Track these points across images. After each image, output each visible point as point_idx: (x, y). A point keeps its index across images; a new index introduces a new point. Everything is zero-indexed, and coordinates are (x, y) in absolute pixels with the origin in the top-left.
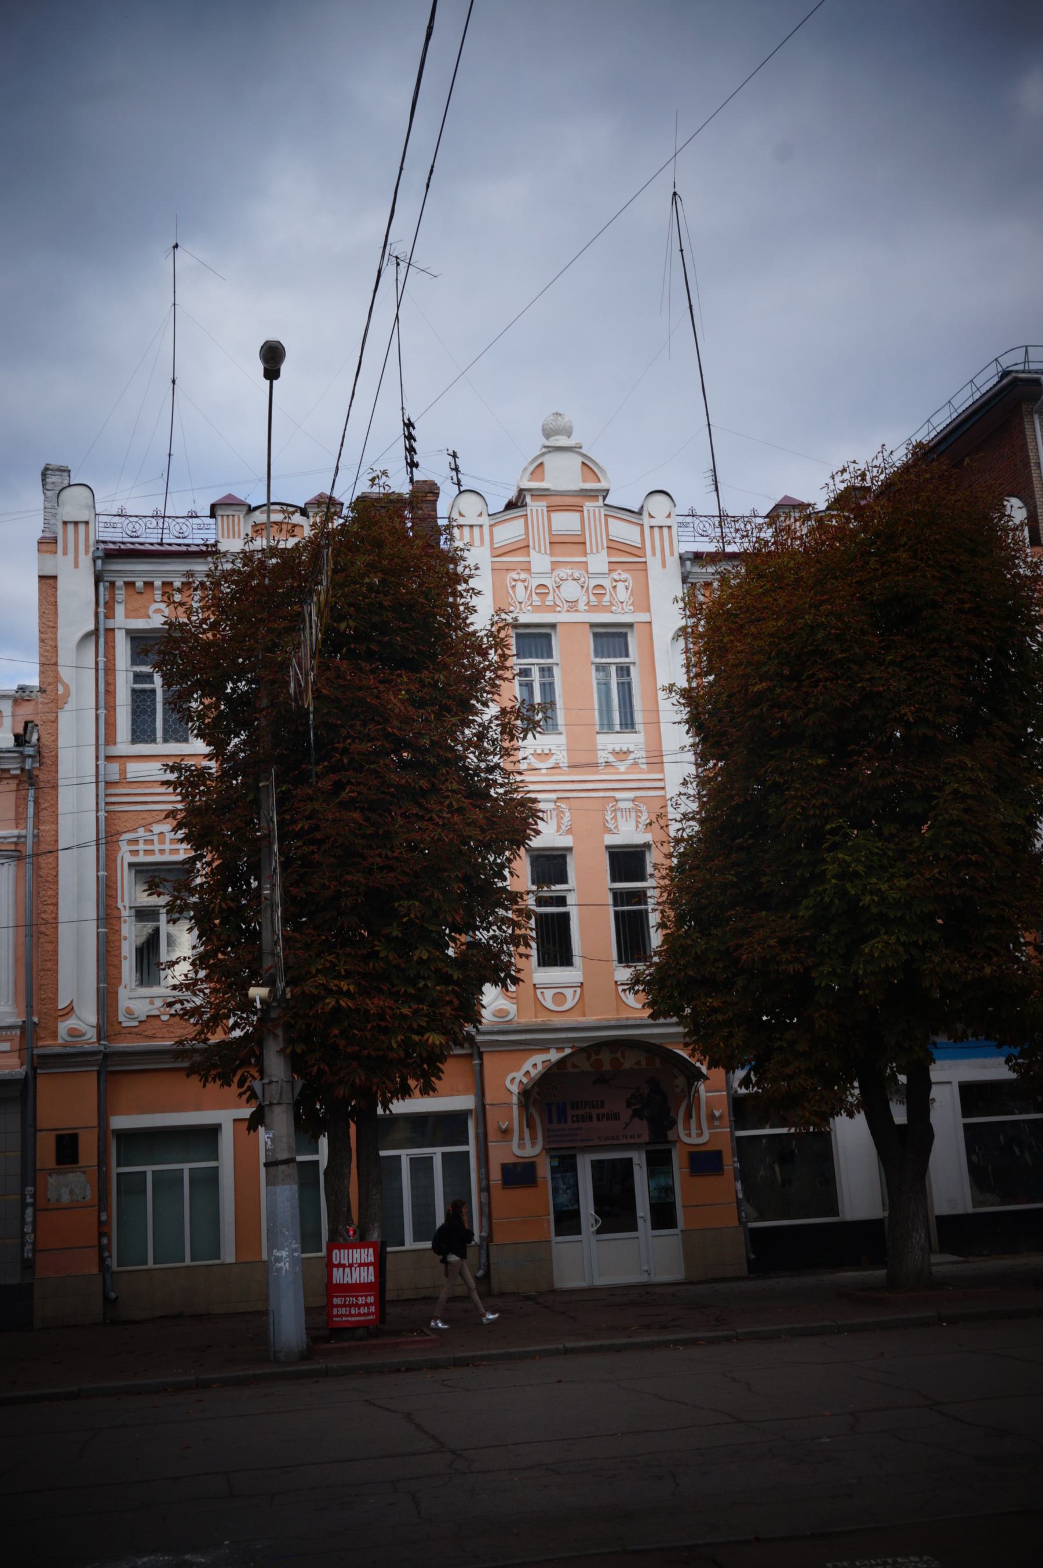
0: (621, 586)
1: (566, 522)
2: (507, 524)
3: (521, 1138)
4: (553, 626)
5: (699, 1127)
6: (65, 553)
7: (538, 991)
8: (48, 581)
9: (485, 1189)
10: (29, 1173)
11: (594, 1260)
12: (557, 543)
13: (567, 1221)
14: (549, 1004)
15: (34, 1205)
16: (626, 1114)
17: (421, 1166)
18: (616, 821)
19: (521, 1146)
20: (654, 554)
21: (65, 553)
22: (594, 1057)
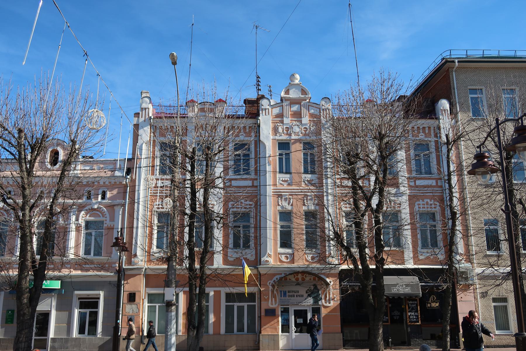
9: (260, 317)
16: (306, 295)
17: (241, 309)
22: (296, 277)
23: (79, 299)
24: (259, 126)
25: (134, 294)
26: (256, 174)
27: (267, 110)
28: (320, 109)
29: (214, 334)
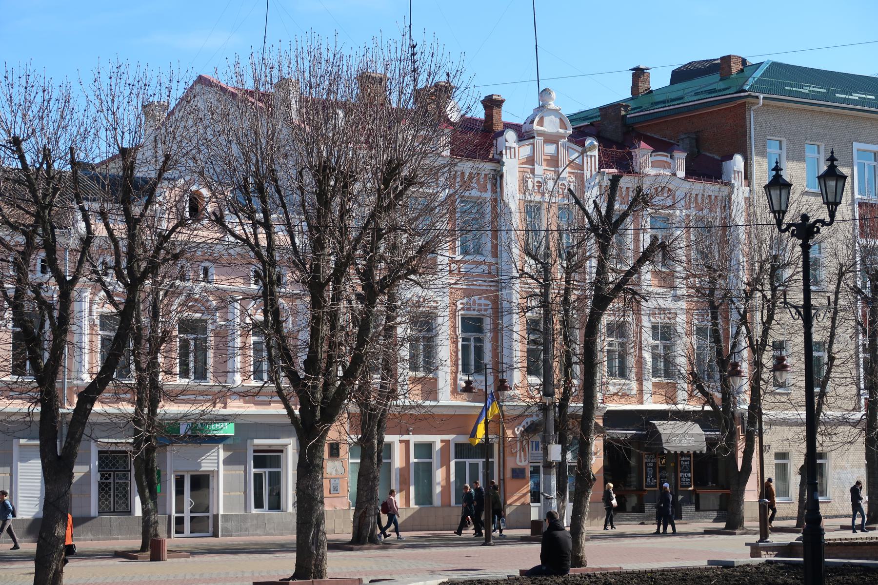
3: (520, 456)
23: (255, 451)
24: (502, 176)
25: (338, 444)
26: (495, 254)
27: (513, 150)
29: (443, 506)
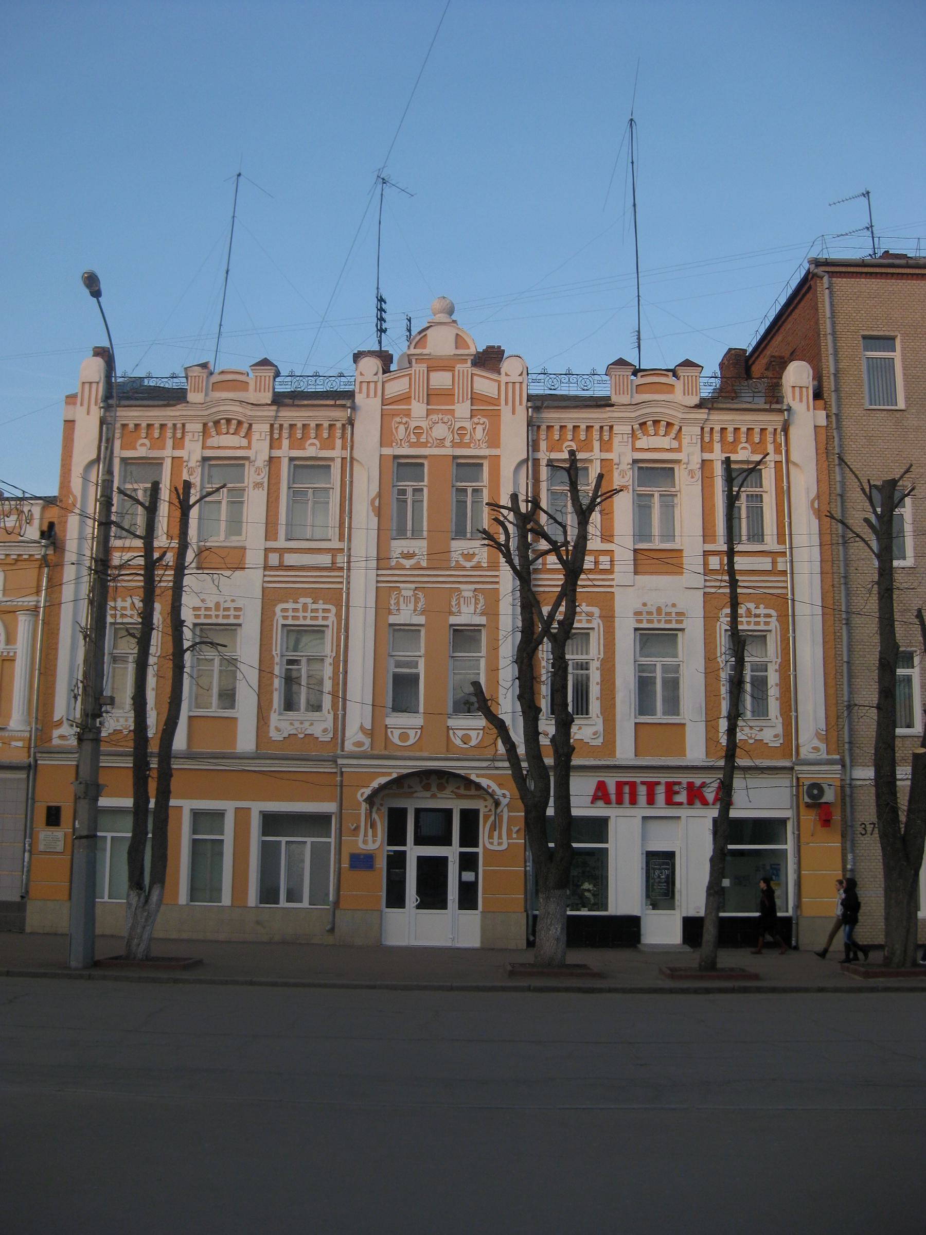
0: (479, 429)
1: (441, 380)
2: (396, 381)
3: (366, 835)
4: (425, 457)
5: (500, 837)
6: (82, 405)
7: (389, 730)
8: (70, 424)
10: (29, 832)
11: (415, 928)
12: (432, 396)
13: (396, 898)
14: (396, 740)
15: (30, 851)
18: (459, 606)
19: (365, 842)
20: (506, 403)
21: (82, 405)
22: (425, 781)
28: (499, 382)
